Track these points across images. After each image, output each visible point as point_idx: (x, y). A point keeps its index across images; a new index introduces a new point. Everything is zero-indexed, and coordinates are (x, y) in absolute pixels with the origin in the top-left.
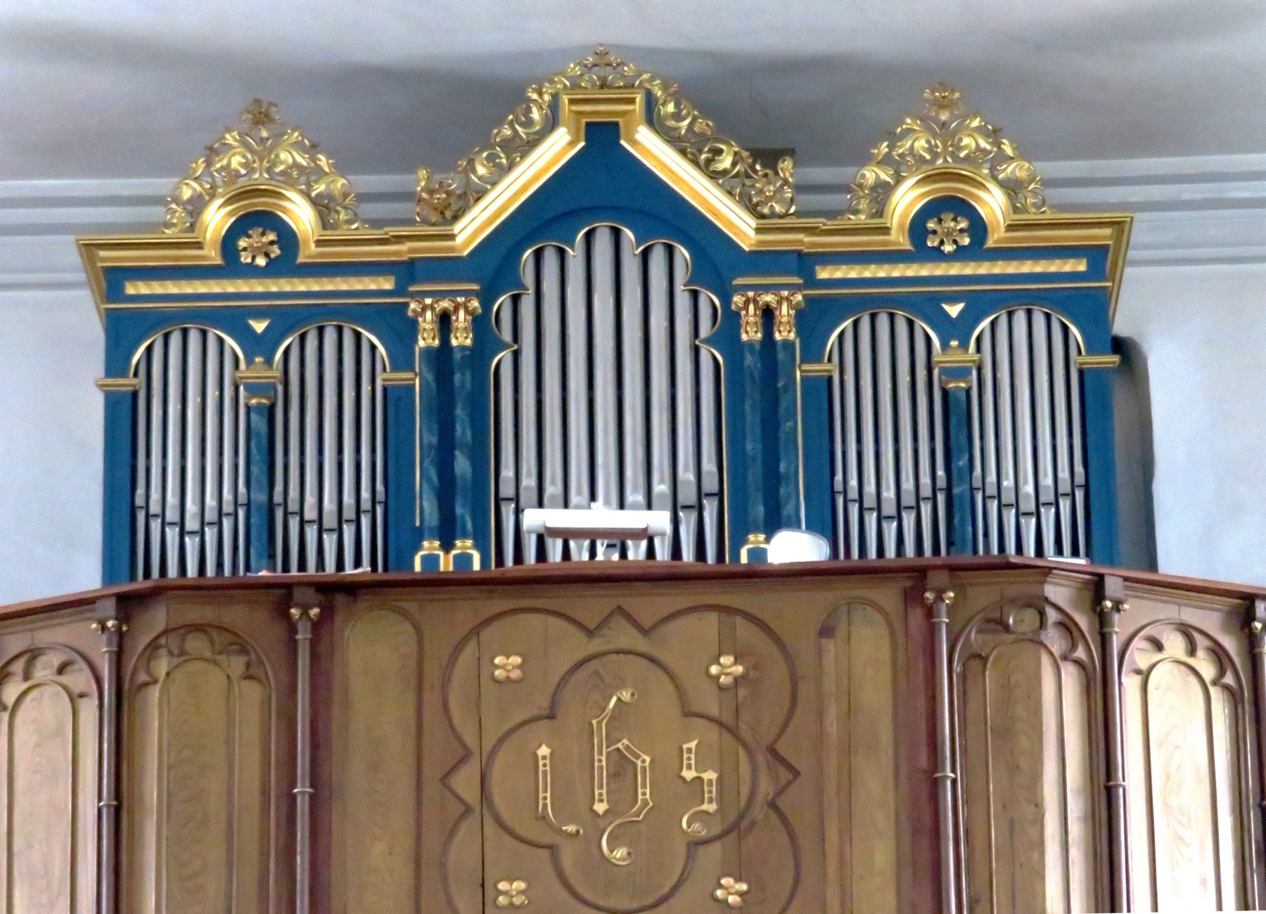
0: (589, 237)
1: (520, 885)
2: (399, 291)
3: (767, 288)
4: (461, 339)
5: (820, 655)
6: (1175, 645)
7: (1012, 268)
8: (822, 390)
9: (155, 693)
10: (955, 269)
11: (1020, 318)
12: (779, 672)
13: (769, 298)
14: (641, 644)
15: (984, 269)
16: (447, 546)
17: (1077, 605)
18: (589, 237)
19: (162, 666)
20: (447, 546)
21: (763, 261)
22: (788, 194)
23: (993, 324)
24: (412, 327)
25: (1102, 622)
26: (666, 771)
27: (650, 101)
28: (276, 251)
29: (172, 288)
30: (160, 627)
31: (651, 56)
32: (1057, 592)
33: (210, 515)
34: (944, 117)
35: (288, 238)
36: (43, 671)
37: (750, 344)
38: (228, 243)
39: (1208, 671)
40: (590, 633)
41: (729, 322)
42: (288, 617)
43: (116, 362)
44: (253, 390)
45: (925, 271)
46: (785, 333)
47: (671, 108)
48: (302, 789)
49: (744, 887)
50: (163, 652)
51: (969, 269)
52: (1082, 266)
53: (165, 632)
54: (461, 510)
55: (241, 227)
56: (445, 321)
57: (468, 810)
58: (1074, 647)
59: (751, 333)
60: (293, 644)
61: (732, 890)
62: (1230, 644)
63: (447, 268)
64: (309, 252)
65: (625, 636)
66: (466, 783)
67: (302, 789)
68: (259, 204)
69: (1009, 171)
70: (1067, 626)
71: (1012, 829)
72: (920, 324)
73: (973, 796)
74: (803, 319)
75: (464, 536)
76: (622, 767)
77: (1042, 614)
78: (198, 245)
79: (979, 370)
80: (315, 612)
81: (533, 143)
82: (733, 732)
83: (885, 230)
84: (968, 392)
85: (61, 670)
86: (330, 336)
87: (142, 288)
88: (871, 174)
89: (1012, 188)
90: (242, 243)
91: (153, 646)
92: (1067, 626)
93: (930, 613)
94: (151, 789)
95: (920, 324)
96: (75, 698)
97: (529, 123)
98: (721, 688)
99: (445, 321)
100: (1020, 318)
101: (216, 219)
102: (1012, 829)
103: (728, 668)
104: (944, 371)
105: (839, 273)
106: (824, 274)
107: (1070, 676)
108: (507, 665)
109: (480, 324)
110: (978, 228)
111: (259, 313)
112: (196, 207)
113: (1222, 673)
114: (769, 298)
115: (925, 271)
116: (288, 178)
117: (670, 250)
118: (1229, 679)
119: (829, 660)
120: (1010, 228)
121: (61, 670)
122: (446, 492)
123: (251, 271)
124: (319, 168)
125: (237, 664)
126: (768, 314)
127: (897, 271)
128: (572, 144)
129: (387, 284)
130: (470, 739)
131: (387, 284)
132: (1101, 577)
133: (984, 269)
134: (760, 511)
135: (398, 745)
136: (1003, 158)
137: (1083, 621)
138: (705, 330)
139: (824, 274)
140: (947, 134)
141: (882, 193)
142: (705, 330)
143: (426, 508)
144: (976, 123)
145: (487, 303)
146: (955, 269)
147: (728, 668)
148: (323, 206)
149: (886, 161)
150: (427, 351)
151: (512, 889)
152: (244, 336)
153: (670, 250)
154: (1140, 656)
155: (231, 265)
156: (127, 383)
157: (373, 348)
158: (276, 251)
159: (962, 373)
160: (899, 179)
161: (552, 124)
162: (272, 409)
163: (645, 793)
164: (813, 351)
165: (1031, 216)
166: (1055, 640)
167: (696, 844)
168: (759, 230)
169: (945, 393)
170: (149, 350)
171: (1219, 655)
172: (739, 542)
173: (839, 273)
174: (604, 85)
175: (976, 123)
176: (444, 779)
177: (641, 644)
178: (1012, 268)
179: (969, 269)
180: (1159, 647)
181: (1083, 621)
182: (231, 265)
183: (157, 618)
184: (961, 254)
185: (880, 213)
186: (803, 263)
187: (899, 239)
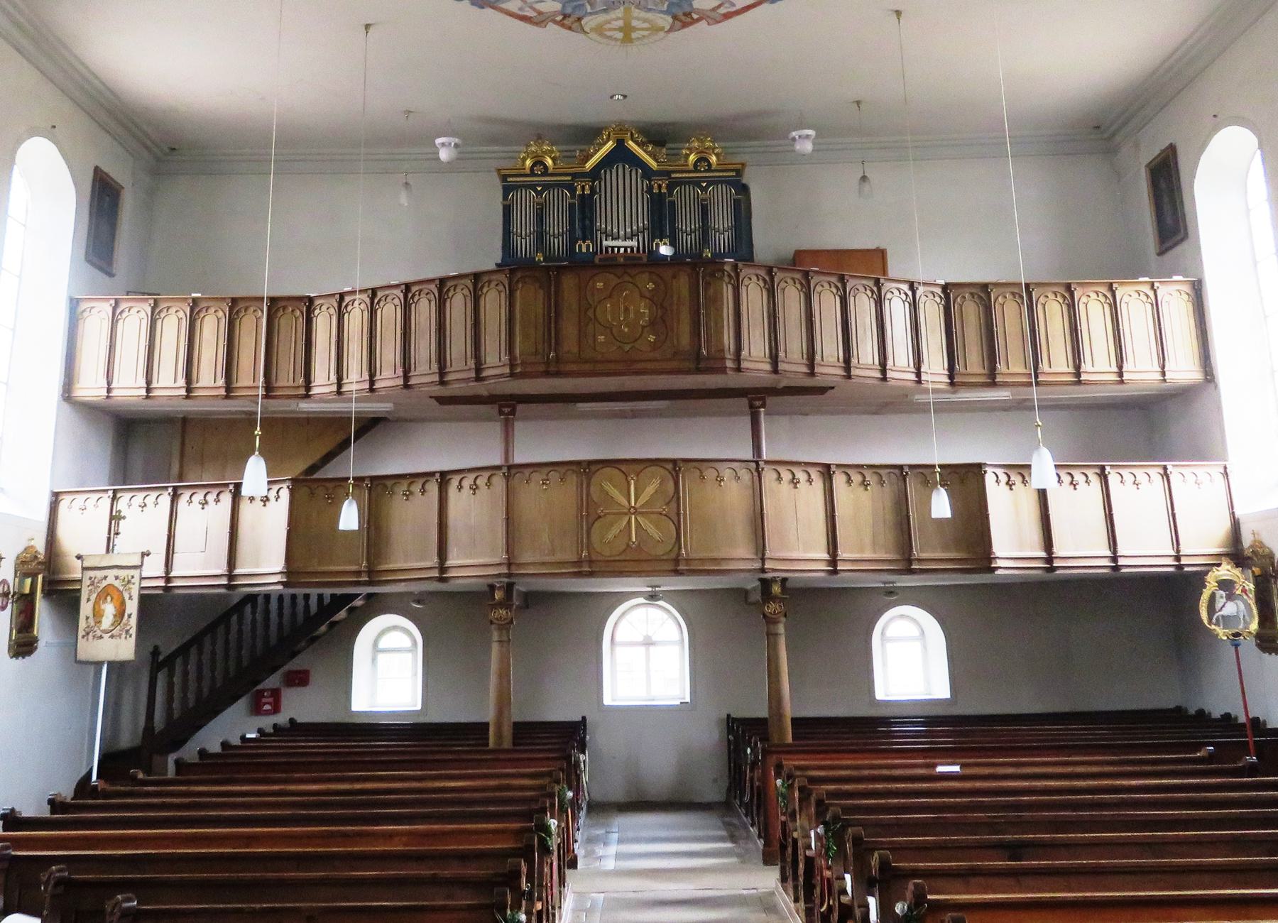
0: (617, 168)
1: (603, 337)
2: (572, 180)
3: (659, 180)
4: (588, 192)
5: (672, 283)
6: (754, 278)
7: (717, 174)
8: (672, 204)
9: (518, 292)
10: (704, 175)
11: (720, 186)
12: (662, 287)
13: (660, 182)
14: (631, 280)
15: (711, 174)
16: (584, 242)
17: (731, 270)
18: (617, 168)
19: (520, 286)
20: (584, 242)
21: (660, 173)
22: (665, 156)
23: (713, 188)
24: (575, 189)
25: (738, 275)
26: (637, 312)
27: (632, 134)
28: (543, 170)
29: (518, 179)
30: (519, 276)
31: (632, 122)
32: (727, 268)
33: (528, 234)
34: (702, 138)
35: (546, 167)
36: (493, 285)
37: (655, 193)
38: (532, 169)
39: (762, 285)
40: (619, 278)
41: (650, 188)
42: (549, 274)
43: (505, 197)
44: (538, 204)
45: (698, 175)
46: (664, 190)
47: (637, 136)
48: (553, 314)
49: (654, 337)
50: (520, 283)
51: (707, 175)
52: (734, 174)
53: (521, 278)
54: (588, 233)
55: (534, 165)
56: (583, 188)
57: (591, 319)
58: (731, 280)
59: (655, 191)
60: (550, 280)
61: (652, 338)
62: (767, 278)
63: (583, 175)
64: (551, 170)
65: (627, 278)
66: (590, 313)
67: (553, 314)
68: (540, 159)
69: (717, 151)
70: (729, 276)
71: (716, 324)
72: (696, 188)
73: (708, 315)
74: (668, 186)
75: (588, 240)
76: (626, 310)
77: (724, 274)
78: (524, 169)
79: (710, 199)
80: (555, 273)
81: (605, 143)
82: (652, 301)
83: (688, 165)
84: (707, 204)
85: (497, 285)
86: (556, 191)
87: (511, 179)
88: (684, 152)
89: (717, 155)
90: (535, 168)
91: (518, 281)
92: (729, 276)
93: (698, 273)
94: (518, 316)
95: (696, 188)
96: (500, 292)
97: (602, 139)
98: (650, 291)
99: (583, 188)
100: (720, 186)
101: (528, 163)
102: (716, 324)
103: (650, 286)
104: (701, 200)
105: (677, 175)
106: (673, 176)
107: (730, 286)
108: (600, 285)
109: (592, 188)
110: (710, 165)
111: (539, 186)
112: (524, 160)
113: (765, 285)
114: (660, 182)
115: (698, 175)
116: (545, 153)
117: (637, 170)
118: (767, 286)
119: (674, 284)
120: (718, 165)
121: (497, 285)
122: (583, 228)
123: (537, 175)
124: (553, 150)
125: (537, 285)
126: (660, 186)
127: (691, 175)
128: (613, 145)
129: (569, 178)
130: (591, 303)
131: (569, 178)
132: (737, 265)
133: (711, 174)
134: (658, 233)
135: (575, 306)
136: (715, 148)
137: (733, 274)
138: (645, 189)
139: (673, 176)
140: (702, 141)
141: (687, 156)
142: (645, 189)
143: (578, 233)
144: (709, 139)
145: (593, 184)
146: (704, 175)
147: (650, 286)
148: (554, 159)
149: (688, 149)
150: (579, 195)
151: (601, 338)
152: (536, 191)
153: (637, 170)
154: (746, 282)
155: (532, 174)
156: (507, 203)
157: (566, 194)
158: (543, 170)
159: (705, 200)
160: (691, 153)
161: (608, 140)
162: (542, 209)
163: (632, 316)
164: (671, 194)
165: (722, 163)
166: (726, 279)
167: (643, 327)
168: (658, 165)
169: (702, 204)
170: (513, 195)
171: (764, 280)
172: (653, 241)
173: (677, 175)
174: (621, 130)
175: (709, 139)
176: (585, 313)
177: (631, 280)
178: (717, 174)
179: (707, 175)
180: (751, 279)
181: (733, 274)
182: (532, 174)
183: (519, 275)
184: (705, 171)
185: (686, 162)
186: (668, 173)
187: (691, 167)
